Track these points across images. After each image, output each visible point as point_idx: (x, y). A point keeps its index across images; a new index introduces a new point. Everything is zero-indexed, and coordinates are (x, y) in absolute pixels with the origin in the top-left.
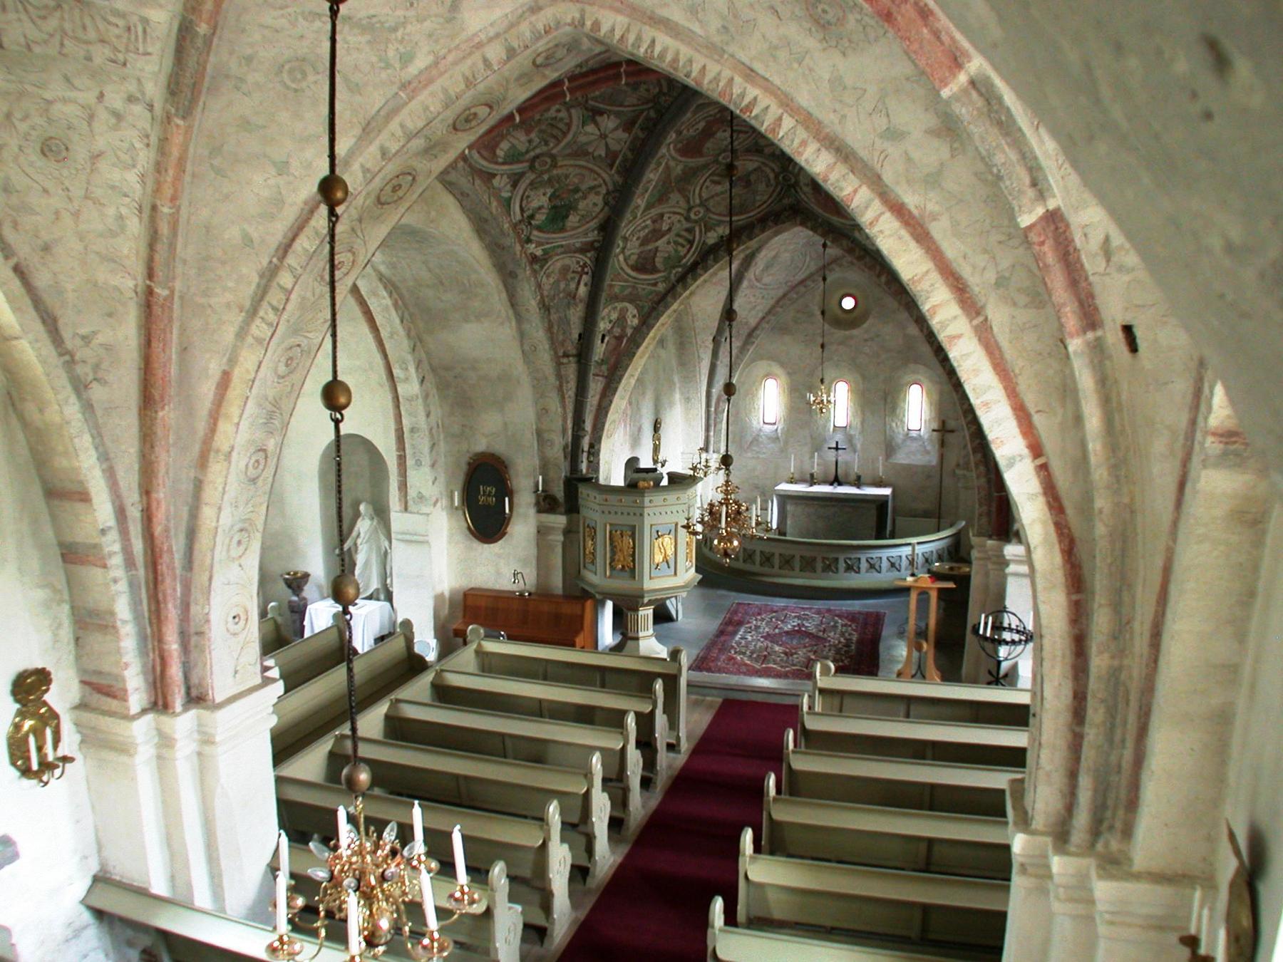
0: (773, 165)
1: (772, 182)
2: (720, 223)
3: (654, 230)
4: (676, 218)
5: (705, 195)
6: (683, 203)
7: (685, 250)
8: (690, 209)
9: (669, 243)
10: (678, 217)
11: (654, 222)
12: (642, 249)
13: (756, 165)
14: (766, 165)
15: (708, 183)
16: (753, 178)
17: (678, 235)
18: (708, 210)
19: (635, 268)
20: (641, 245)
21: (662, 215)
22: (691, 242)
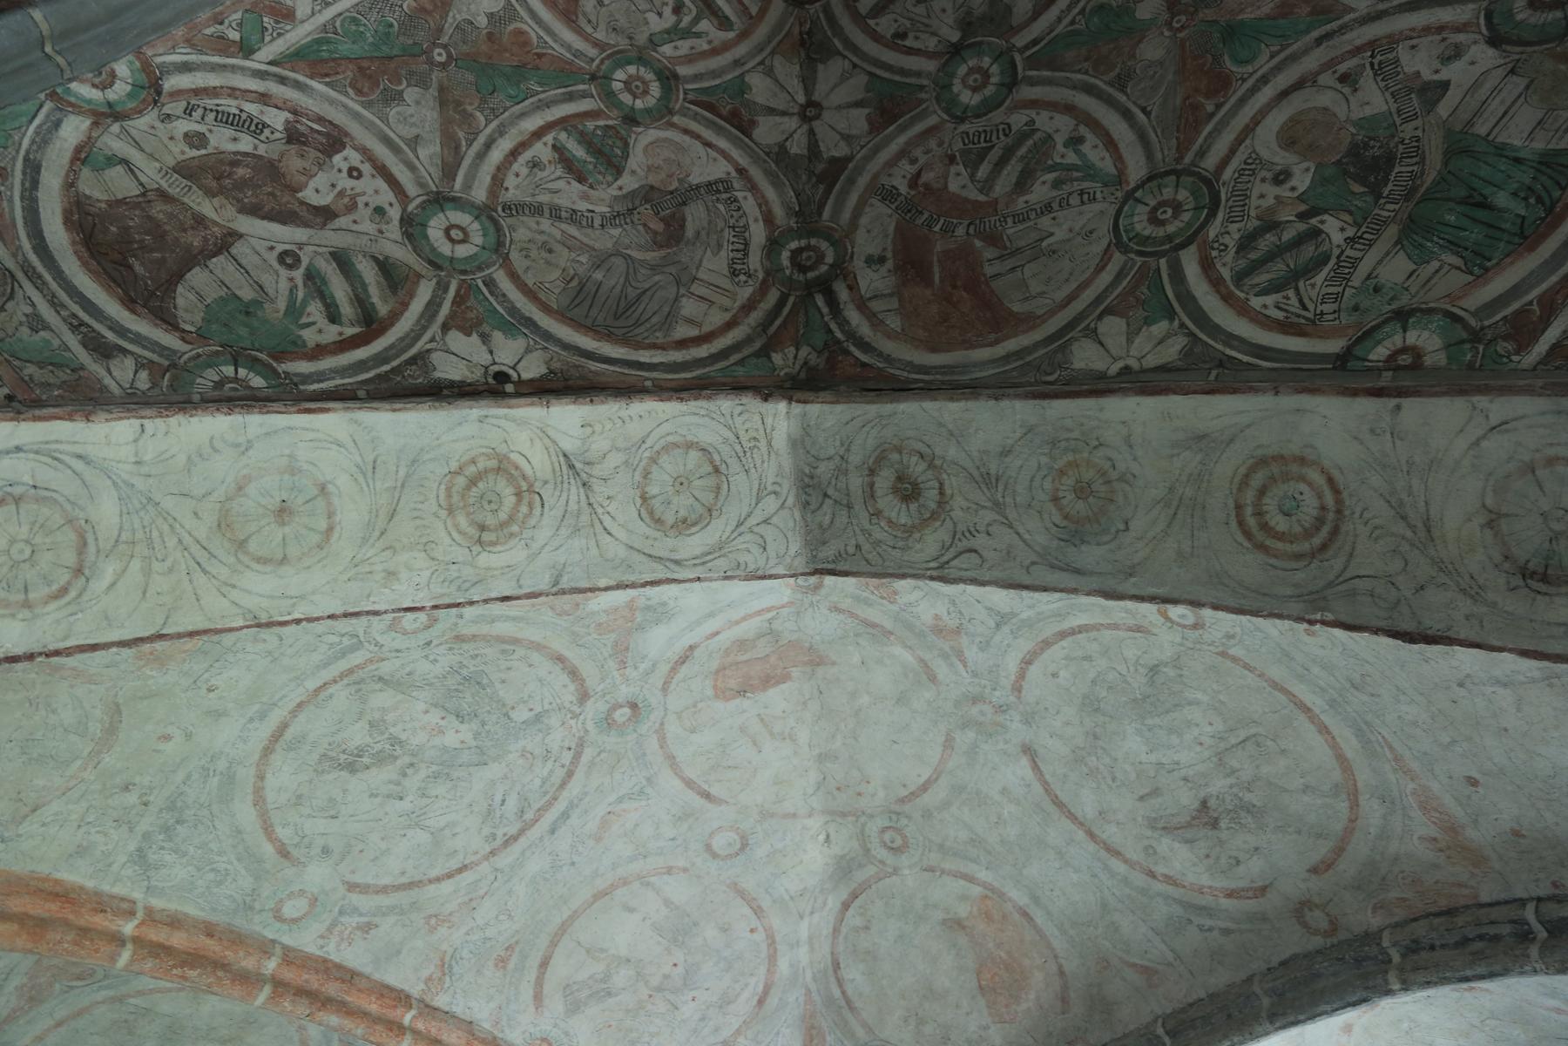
0: (770, 193)
1: (755, 260)
2: (517, 324)
3: (271, 169)
4: (373, 190)
5: (514, 188)
6: (429, 153)
7: (331, 333)
8: (439, 200)
9: (288, 259)
10: (386, 196)
11: (293, 136)
12: (176, 186)
13: (721, 169)
14: (753, 188)
15: (541, 150)
16: (695, 215)
17: (341, 260)
18: (499, 248)
19: (85, 222)
20: (184, 170)
21: (335, 141)
22: (372, 326)
